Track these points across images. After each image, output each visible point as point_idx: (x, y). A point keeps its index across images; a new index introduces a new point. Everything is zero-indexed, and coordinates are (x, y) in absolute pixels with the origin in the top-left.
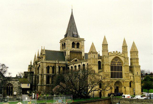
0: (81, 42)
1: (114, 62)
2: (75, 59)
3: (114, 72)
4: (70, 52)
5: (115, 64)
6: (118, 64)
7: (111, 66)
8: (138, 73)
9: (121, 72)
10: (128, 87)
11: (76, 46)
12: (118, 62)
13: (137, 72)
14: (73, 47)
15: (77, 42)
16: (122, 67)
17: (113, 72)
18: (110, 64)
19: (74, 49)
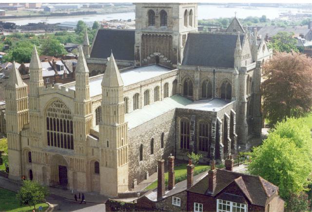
0: (170, 9)
1: (54, 110)
2: (156, 54)
3: (53, 132)
4: (143, 35)
5: (56, 115)
6: (63, 116)
7: (48, 118)
8: (109, 144)
9: (70, 134)
10: (81, 174)
11: (158, 21)
12: (64, 112)
13: (108, 142)
14: (151, 21)
15: (160, 10)
16: (71, 122)
17: (52, 133)
18: (42, 114)
19: (153, 27)
